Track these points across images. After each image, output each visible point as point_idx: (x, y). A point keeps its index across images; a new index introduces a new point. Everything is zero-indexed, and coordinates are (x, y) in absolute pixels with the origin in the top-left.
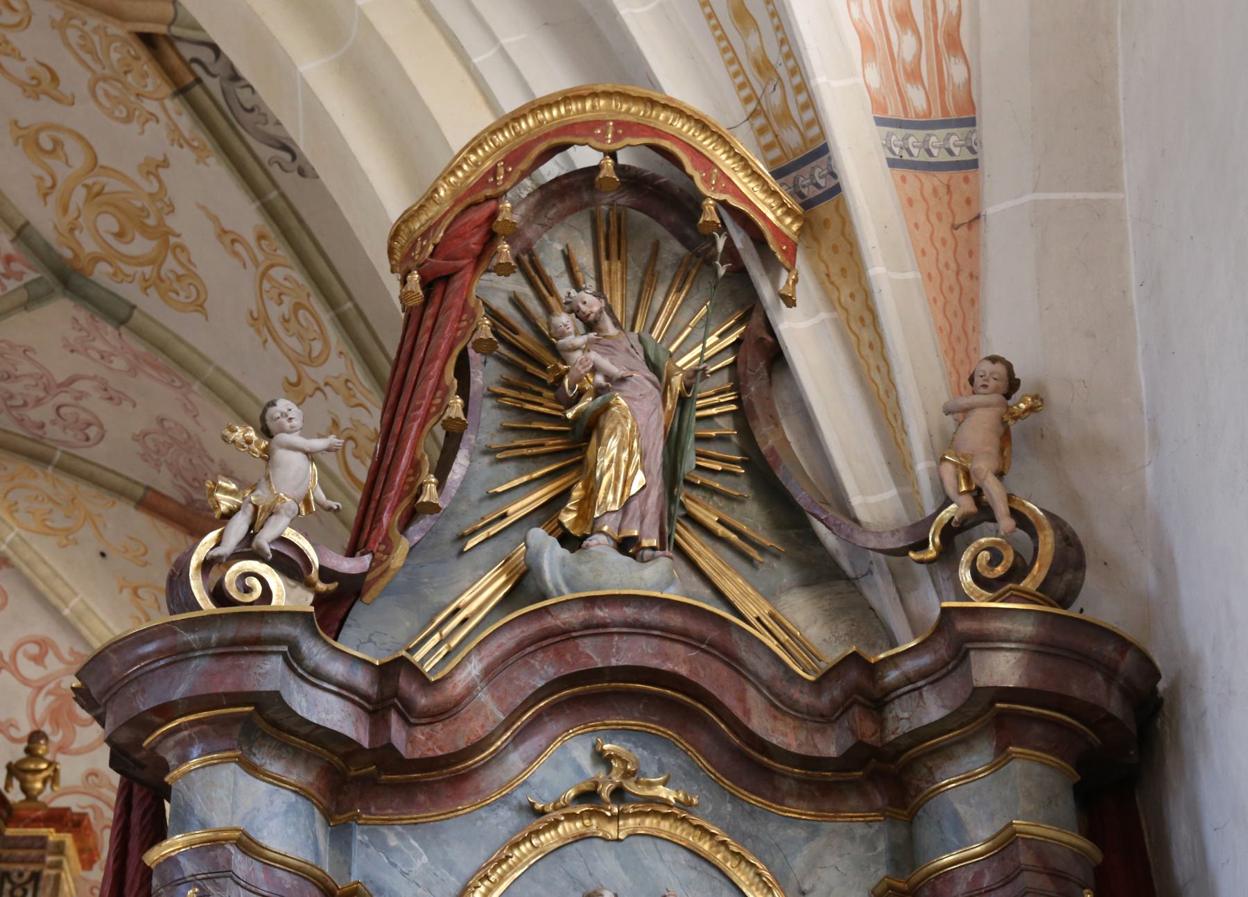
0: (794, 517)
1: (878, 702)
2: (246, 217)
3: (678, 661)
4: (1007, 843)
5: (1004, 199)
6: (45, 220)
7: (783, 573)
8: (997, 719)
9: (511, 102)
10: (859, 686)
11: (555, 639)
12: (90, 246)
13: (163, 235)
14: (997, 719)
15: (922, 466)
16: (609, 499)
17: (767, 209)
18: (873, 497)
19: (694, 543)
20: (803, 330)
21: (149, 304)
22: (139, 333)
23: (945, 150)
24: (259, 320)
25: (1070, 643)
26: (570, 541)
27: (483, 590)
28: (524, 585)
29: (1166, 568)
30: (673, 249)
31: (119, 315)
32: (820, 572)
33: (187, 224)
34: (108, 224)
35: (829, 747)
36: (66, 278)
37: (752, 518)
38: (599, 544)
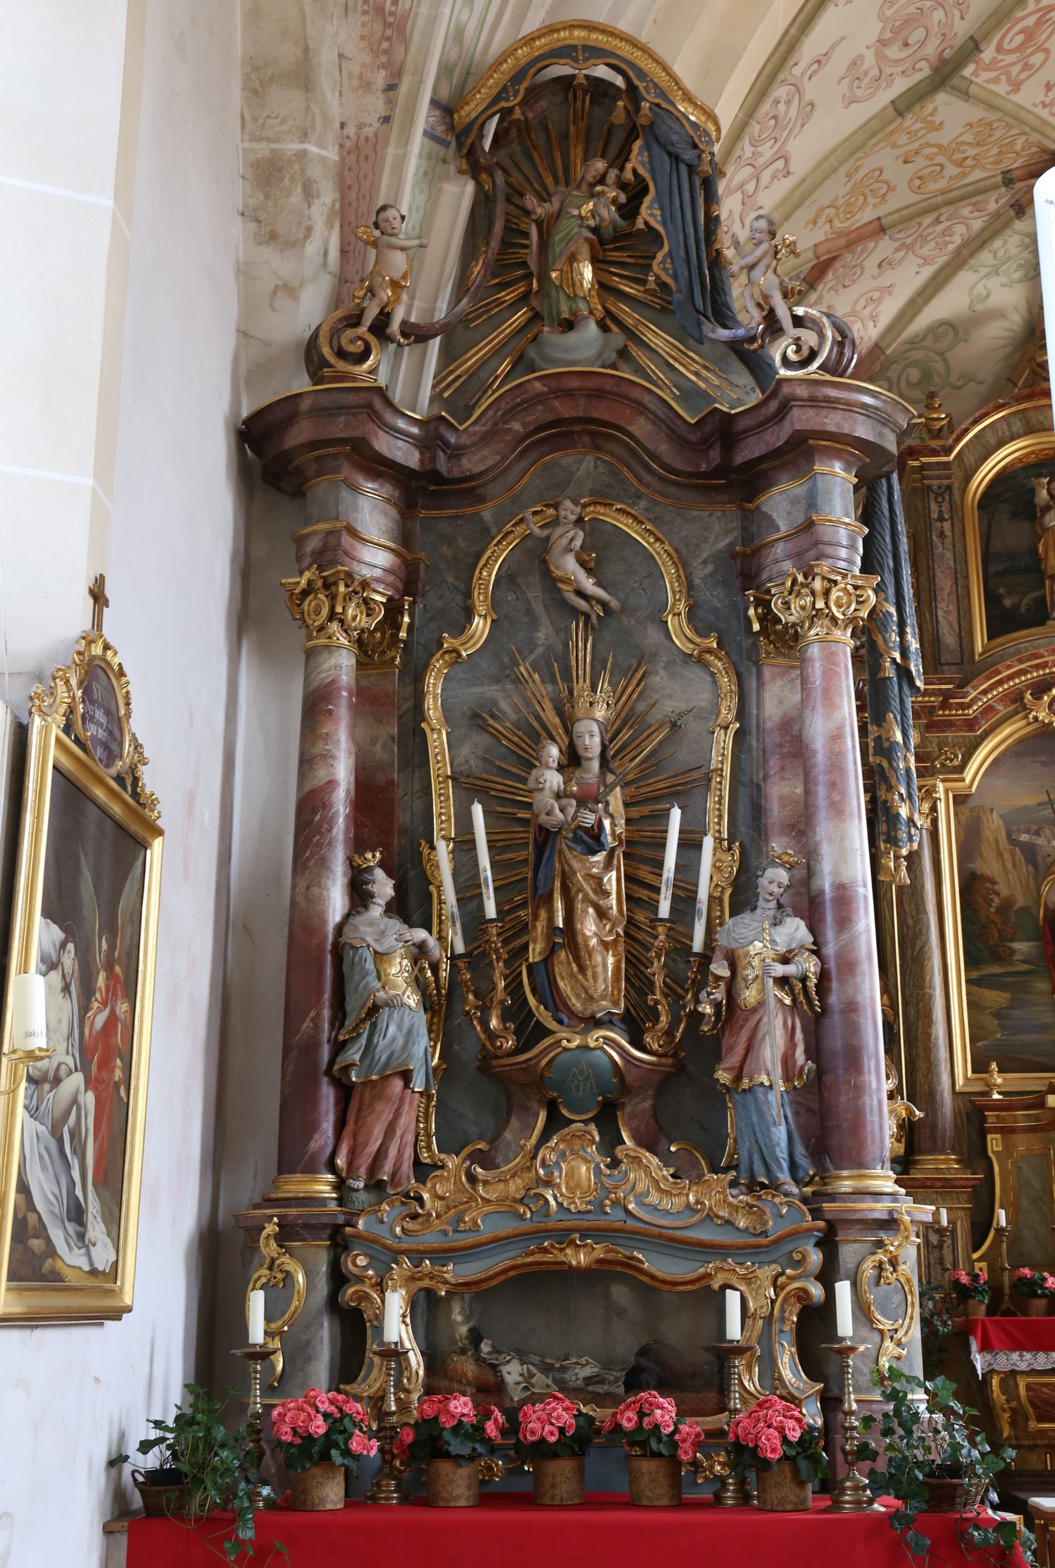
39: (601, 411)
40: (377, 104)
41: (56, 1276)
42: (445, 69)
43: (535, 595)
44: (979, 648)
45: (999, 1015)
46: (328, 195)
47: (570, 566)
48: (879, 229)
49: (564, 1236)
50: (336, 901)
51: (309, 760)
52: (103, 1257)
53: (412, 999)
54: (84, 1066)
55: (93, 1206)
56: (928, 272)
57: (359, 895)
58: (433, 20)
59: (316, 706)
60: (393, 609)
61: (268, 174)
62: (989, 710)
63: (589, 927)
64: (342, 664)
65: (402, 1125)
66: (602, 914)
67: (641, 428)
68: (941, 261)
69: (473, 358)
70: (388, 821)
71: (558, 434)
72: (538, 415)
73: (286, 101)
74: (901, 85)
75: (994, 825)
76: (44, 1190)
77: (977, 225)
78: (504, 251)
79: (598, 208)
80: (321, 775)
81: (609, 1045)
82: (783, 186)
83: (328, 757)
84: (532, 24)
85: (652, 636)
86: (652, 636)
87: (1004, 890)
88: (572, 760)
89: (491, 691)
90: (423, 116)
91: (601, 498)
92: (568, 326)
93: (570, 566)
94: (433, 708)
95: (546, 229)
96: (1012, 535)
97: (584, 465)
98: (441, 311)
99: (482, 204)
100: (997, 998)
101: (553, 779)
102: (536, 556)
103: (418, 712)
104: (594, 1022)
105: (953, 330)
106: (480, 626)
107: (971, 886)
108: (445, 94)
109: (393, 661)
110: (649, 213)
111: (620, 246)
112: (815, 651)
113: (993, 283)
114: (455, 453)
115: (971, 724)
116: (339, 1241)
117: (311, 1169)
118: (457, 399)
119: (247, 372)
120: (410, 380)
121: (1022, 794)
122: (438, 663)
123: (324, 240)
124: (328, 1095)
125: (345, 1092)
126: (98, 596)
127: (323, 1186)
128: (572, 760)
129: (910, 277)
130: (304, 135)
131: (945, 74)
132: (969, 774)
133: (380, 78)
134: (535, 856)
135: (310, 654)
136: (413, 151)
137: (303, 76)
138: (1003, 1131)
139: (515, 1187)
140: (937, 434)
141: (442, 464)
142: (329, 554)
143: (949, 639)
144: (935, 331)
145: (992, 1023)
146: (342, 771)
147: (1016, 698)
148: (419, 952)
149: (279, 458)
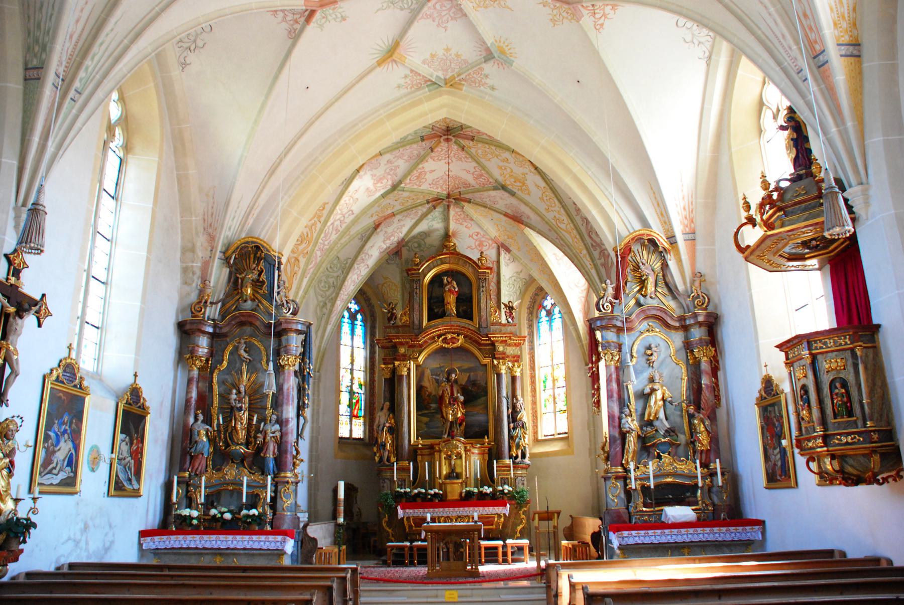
0: (671, 290)
1: (685, 320)
2: (542, 184)
3: (659, 313)
4: (701, 339)
5: (699, 247)
6: (501, 179)
7: (670, 298)
8: (700, 324)
9: (632, 231)
10: (682, 319)
11: (643, 311)
12: (508, 183)
13: (524, 184)
14: (700, 324)
15: (688, 285)
16: (649, 291)
17: (667, 246)
18: (681, 287)
19: (658, 294)
20: (672, 264)
21: (519, 193)
22: (517, 197)
23: (692, 236)
24: (542, 199)
25: (709, 315)
26: (644, 296)
27: (633, 302)
28: (638, 304)
29: (719, 299)
30: (652, 248)
31: (513, 194)
32: (674, 298)
33: (528, 182)
34: (513, 180)
35: (677, 324)
36: (504, 188)
37: (665, 290)
38: (648, 297)
39: (250, 319)
40: (209, 253)
41: (125, 490)
42: (224, 245)
43: (236, 357)
44: (424, 324)
45: (426, 424)
46: (198, 273)
47: (242, 352)
48: (393, 215)
49: (228, 484)
50: (191, 420)
51: (188, 392)
52: (136, 486)
53: (205, 439)
54: (131, 456)
55: (133, 478)
56: (414, 221)
57: (196, 419)
58: (219, 238)
59: (190, 381)
60: (207, 360)
61: (185, 270)
62: (425, 342)
63: (239, 426)
64: (195, 373)
65: (201, 463)
66: (242, 424)
67: (258, 323)
68: (417, 218)
69: (228, 305)
70: (204, 402)
71: (242, 324)
72: (238, 320)
73: (189, 255)
74: (382, 191)
75: (428, 372)
76: (122, 476)
77: (425, 210)
78: (235, 285)
79: (252, 276)
80: (189, 395)
81: (242, 450)
82: (352, 217)
83: (191, 392)
84: (243, 236)
85: (259, 365)
86: (259, 365)
87: (429, 390)
88: (239, 392)
89: (227, 377)
90: (218, 255)
91: (251, 336)
92: (246, 301)
93: (242, 352)
94: (215, 380)
95: (243, 280)
96: (437, 292)
97: (248, 329)
98: (221, 296)
99: (230, 273)
100: (426, 419)
101: (234, 396)
102: (236, 349)
103: (212, 382)
104: (238, 444)
105: (425, 234)
106: (225, 363)
107: (420, 389)
108: (224, 249)
109: (206, 373)
110: (263, 277)
111: (257, 284)
112: (286, 372)
113: (434, 223)
114: (221, 328)
115: (421, 346)
116: (188, 485)
117: (185, 471)
118: (223, 315)
119: (181, 310)
120: (213, 312)
121: (434, 364)
122: (216, 371)
123: (197, 282)
124: (188, 458)
125: (192, 457)
126: (136, 375)
127: (187, 474)
128: (239, 392)
129: (408, 223)
130: (193, 262)
131: (394, 187)
132: (420, 359)
133: (209, 249)
134: (230, 412)
135: (189, 371)
136: (217, 263)
137: (193, 250)
138: (422, 455)
139: (221, 475)
140: (417, 265)
141: (218, 331)
142: (193, 353)
143: (416, 322)
144: (420, 234)
145: (424, 426)
146: (194, 395)
147: (434, 338)
148: (207, 431)
149: (186, 330)
